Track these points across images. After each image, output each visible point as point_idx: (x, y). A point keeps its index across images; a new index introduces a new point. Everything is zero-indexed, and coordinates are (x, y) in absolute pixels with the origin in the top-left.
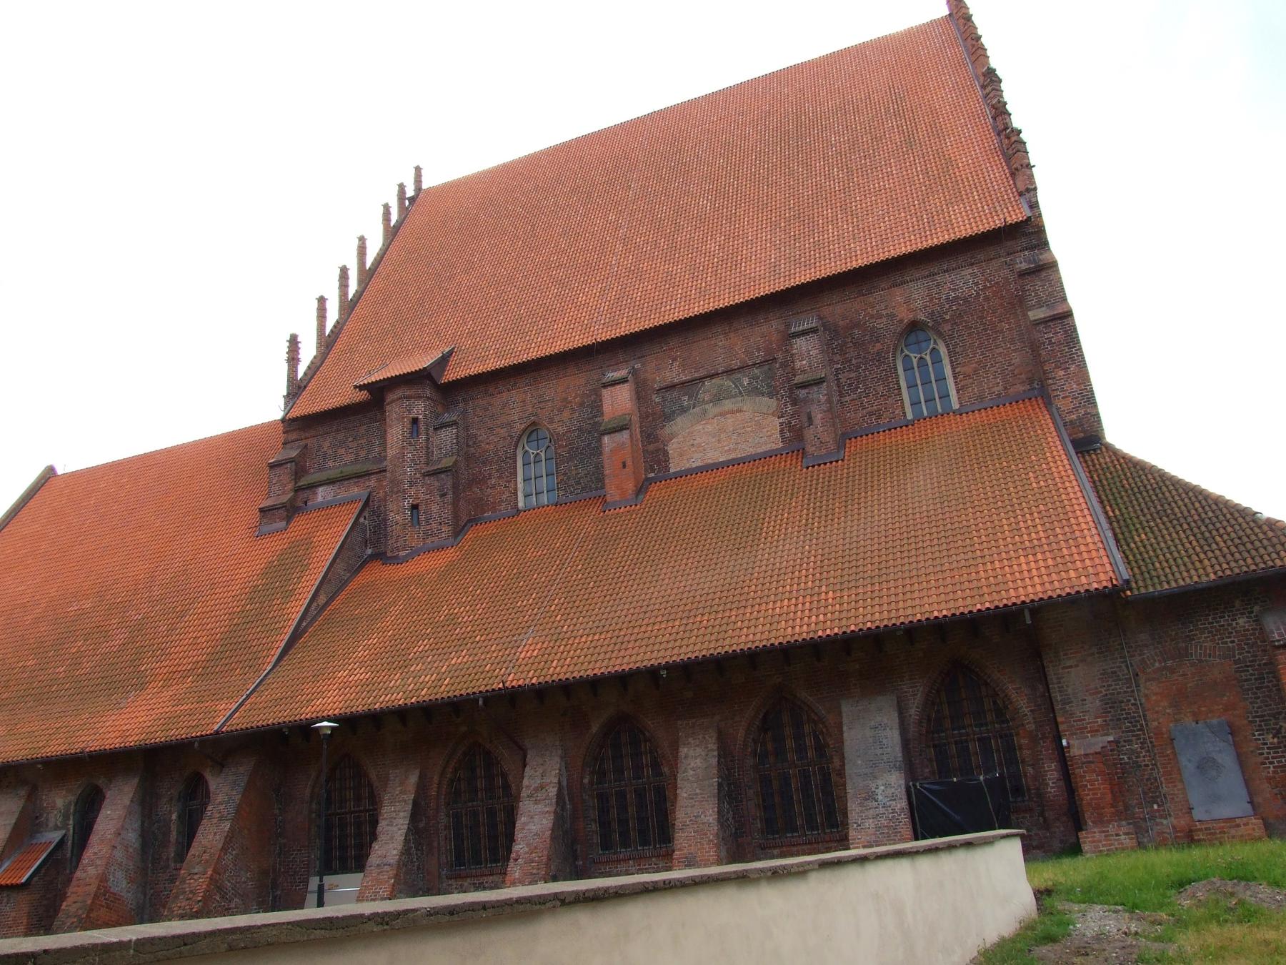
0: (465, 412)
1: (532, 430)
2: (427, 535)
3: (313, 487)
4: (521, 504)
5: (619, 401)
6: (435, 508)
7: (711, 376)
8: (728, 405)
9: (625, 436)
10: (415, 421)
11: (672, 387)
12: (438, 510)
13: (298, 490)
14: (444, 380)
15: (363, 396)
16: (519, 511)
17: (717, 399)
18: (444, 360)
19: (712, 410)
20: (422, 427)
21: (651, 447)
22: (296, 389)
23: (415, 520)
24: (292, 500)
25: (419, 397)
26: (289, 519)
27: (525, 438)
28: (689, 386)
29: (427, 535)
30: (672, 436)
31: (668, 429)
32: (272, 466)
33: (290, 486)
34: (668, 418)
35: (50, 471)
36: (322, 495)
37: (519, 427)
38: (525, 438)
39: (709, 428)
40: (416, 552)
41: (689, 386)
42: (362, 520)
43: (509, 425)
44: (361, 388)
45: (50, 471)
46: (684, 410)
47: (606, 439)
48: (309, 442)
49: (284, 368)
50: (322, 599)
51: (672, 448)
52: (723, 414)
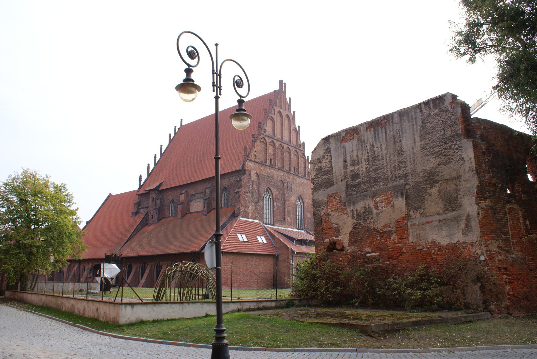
0: (163, 196)
1: (173, 201)
2: (154, 221)
3: (140, 209)
4: (170, 215)
5: (182, 197)
6: (155, 216)
7: (197, 194)
8: (199, 200)
9: (181, 205)
10: (154, 198)
11: (192, 195)
12: (156, 217)
13: (138, 209)
14: (159, 190)
15: (147, 191)
16: (169, 217)
17: (197, 199)
18: (160, 186)
19: (197, 201)
20: (155, 199)
21: (188, 207)
22: (140, 186)
23: (152, 218)
24: (137, 211)
25: (154, 193)
26: (136, 215)
27: (172, 202)
28: (194, 195)
29: (154, 221)
30: (191, 205)
31: (190, 204)
32: (135, 204)
33: (137, 208)
34: (191, 201)
35: (110, 194)
36: (141, 210)
37: (171, 200)
38: (172, 202)
39: (196, 204)
40: (152, 224)
41: (194, 195)
42: (146, 217)
43: (169, 199)
44: (146, 191)
45: (110, 194)
46: (193, 200)
47: (179, 206)
48: (141, 198)
49: (138, 182)
50: (135, 233)
51: (191, 208)
52: (198, 202)
